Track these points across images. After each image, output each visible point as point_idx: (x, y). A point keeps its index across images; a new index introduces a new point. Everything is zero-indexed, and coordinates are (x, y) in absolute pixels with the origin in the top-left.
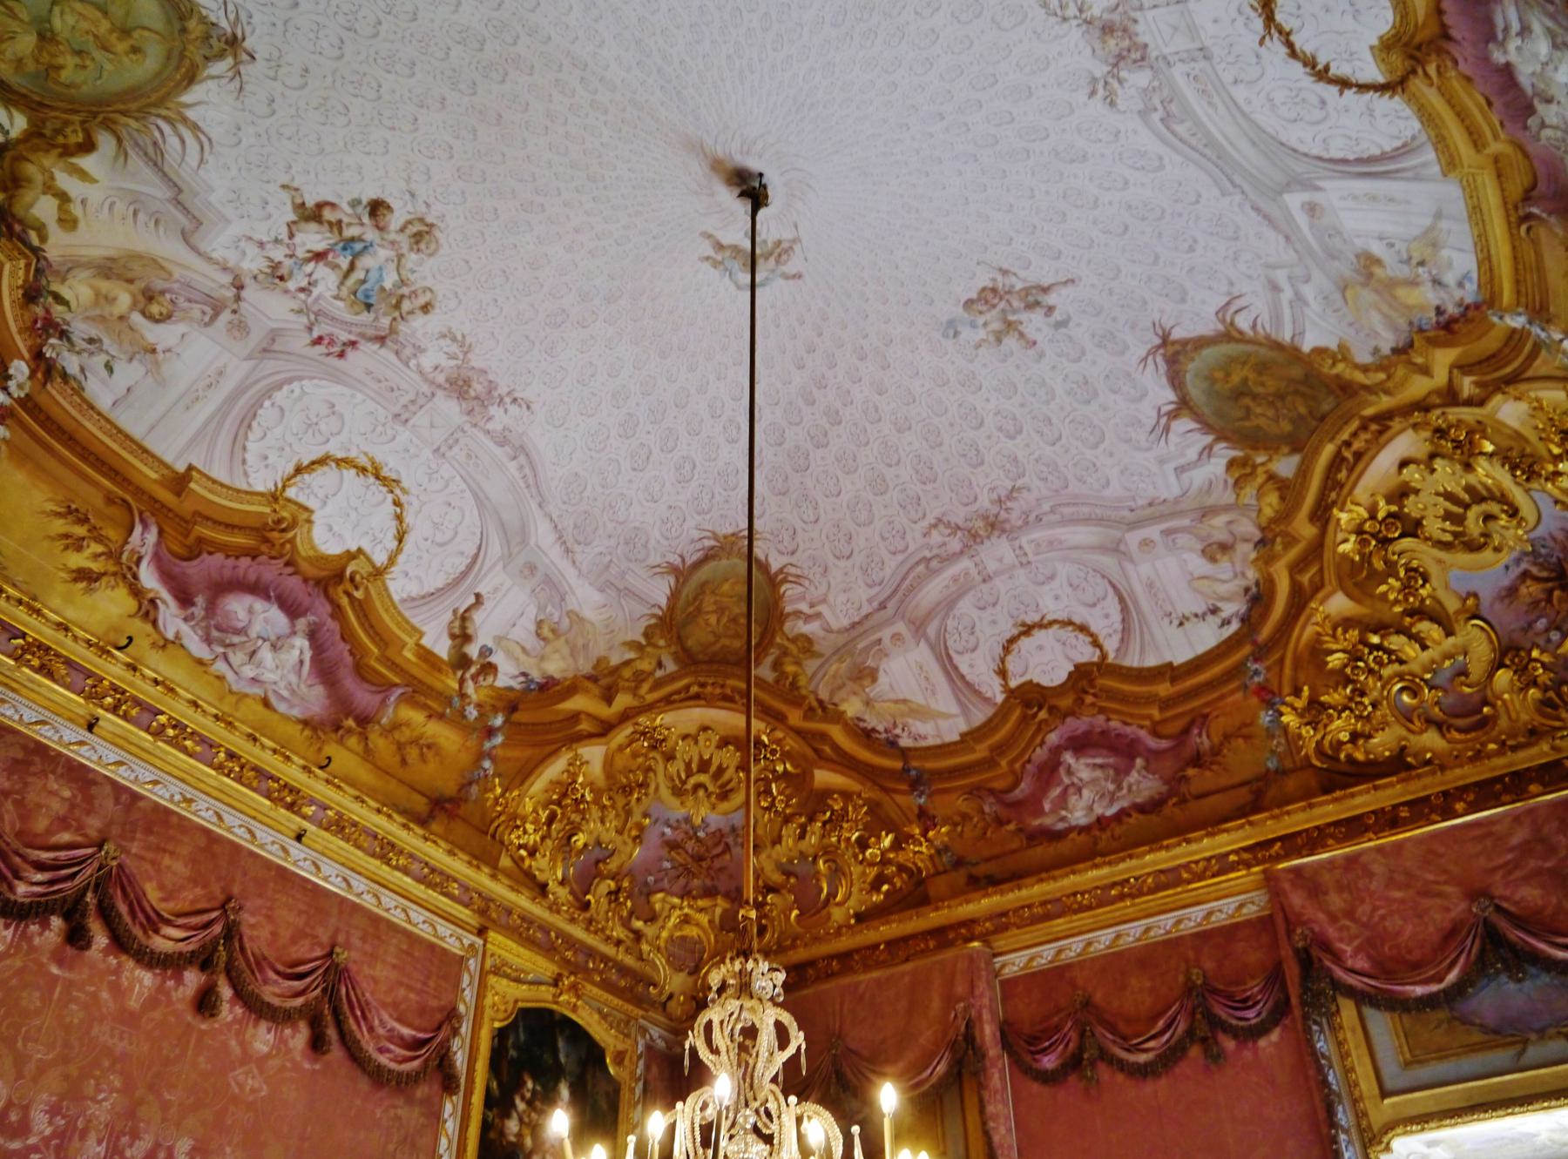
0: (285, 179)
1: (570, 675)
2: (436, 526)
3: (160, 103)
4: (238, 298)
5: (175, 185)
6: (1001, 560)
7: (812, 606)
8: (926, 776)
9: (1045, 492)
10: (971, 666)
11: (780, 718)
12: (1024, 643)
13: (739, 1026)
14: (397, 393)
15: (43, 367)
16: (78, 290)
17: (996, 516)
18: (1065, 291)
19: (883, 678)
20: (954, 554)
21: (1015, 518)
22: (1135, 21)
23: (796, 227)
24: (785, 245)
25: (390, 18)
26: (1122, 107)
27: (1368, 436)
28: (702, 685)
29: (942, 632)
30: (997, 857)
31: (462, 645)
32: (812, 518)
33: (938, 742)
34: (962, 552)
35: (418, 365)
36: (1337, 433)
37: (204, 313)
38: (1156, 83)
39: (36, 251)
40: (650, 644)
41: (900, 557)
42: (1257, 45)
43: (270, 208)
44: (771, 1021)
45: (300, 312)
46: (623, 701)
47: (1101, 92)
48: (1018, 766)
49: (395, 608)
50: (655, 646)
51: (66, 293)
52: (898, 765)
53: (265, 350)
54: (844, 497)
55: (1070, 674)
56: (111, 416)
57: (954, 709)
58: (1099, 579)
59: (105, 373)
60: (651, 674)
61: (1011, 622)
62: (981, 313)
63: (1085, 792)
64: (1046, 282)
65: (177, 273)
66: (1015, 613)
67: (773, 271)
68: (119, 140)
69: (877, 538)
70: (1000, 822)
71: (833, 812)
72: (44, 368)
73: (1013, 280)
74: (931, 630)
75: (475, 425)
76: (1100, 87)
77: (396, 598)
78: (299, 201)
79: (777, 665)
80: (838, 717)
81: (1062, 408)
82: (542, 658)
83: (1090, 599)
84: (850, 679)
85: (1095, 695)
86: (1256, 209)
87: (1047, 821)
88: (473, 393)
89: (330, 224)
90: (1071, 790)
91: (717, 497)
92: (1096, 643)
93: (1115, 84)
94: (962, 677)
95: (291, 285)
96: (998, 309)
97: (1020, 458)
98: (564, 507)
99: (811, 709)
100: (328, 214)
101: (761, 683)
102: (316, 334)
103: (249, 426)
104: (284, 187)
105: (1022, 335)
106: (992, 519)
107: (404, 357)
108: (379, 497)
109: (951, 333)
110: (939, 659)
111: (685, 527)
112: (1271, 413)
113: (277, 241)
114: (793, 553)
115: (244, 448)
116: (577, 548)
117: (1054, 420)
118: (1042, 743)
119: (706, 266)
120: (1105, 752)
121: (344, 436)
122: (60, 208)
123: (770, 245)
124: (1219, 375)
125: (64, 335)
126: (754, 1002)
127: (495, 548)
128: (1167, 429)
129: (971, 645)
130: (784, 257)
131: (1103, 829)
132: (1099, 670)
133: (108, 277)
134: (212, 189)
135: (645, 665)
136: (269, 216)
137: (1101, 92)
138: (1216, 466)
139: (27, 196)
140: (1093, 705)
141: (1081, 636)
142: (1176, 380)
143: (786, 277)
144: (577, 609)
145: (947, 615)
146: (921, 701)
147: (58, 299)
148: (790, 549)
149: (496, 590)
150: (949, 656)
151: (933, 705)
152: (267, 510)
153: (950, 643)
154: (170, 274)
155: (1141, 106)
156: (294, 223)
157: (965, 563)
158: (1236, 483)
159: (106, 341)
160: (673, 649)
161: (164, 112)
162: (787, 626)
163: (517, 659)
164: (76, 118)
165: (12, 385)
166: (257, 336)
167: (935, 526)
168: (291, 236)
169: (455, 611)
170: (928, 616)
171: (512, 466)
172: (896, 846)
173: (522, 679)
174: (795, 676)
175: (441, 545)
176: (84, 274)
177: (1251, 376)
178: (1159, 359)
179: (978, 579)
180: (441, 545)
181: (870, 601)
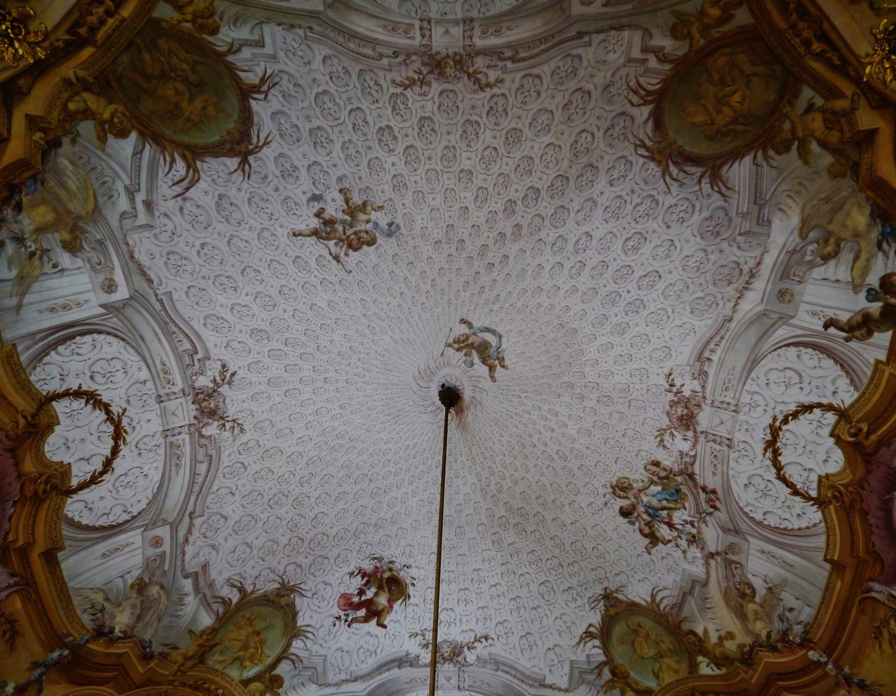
0: (646, 555)
1: (862, 196)
2: (788, 386)
3: (653, 611)
4: (718, 554)
5: (684, 596)
6: (447, 32)
7: (644, 61)
9: (381, 74)
14: (716, 453)
15: (806, 643)
16: (760, 628)
17: (431, 72)
18: (302, 227)
20: (485, 55)
21: (416, 63)
22: (195, 417)
23: (442, 354)
24: (456, 346)
25: (542, 557)
26: (219, 363)
27: (91, 19)
28: (807, 43)
31: (874, 321)
32: (584, 135)
34: (478, 53)
35: (691, 450)
36: (118, 27)
37: (736, 568)
38: (194, 378)
39: (752, 648)
40: (794, 136)
41: (535, 71)
42: (128, 408)
43: (664, 555)
45: (705, 522)
47: (228, 375)
50: (793, 129)
51: (764, 633)
53: (737, 532)
54: (547, 140)
56: (817, 607)
59: (795, 612)
60: (823, 110)
62: (367, 232)
64: (312, 240)
65: (724, 585)
67: (474, 334)
68: (681, 622)
69: (543, 95)
72: (806, 643)
73: (334, 250)
75: (704, 397)
76: (228, 378)
77: (856, 395)
78: (651, 545)
79: (726, 18)
81: (340, 132)
82: (856, 235)
86: (150, 281)
88: (686, 411)
89: (650, 528)
91: (637, 200)
93: (218, 378)
95: (694, 531)
96: (354, 229)
97: (390, 109)
98: (721, 303)
100: (647, 530)
102: (712, 510)
103: (785, 529)
104: (649, 554)
105: (347, 201)
106: (437, 71)
107: (692, 460)
108: (788, 435)
109: (393, 228)
111: (674, 201)
112: (175, 60)
113: (677, 546)
115: (800, 529)
116: (746, 269)
117: (350, 126)
119: (507, 363)
121: (759, 472)
122: (727, 640)
123: (464, 351)
124: (211, 110)
125: (785, 633)
127: (782, 333)
128: (263, 80)
130: (462, 338)
133: (746, 616)
134: (675, 581)
135: (817, 124)
136: (668, 554)
137: (228, 375)
138: (227, 35)
139: (729, 653)
142: (247, 117)
143: (470, 325)
144: (796, 232)
147: (769, 636)
148: (622, 118)
149: (814, 314)
152: (832, 507)
154: (726, 588)
155: (207, 363)
156: (662, 543)
157: (480, 42)
158: (212, 15)
159: (778, 613)
160: (787, 109)
161: (656, 609)
163: (868, 260)
164: (684, 640)
165: (823, 659)
166: (732, 539)
167: (489, 85)
168: (670, 541)
169: (848, 340)
171: (715, 358)
173: (885, 246)
175: (800, 376)
176: (751, 627)
177: (184, 104)
178: (255, 140)
179: (476, 25)
180: (800, 376)
181: (589, 44)
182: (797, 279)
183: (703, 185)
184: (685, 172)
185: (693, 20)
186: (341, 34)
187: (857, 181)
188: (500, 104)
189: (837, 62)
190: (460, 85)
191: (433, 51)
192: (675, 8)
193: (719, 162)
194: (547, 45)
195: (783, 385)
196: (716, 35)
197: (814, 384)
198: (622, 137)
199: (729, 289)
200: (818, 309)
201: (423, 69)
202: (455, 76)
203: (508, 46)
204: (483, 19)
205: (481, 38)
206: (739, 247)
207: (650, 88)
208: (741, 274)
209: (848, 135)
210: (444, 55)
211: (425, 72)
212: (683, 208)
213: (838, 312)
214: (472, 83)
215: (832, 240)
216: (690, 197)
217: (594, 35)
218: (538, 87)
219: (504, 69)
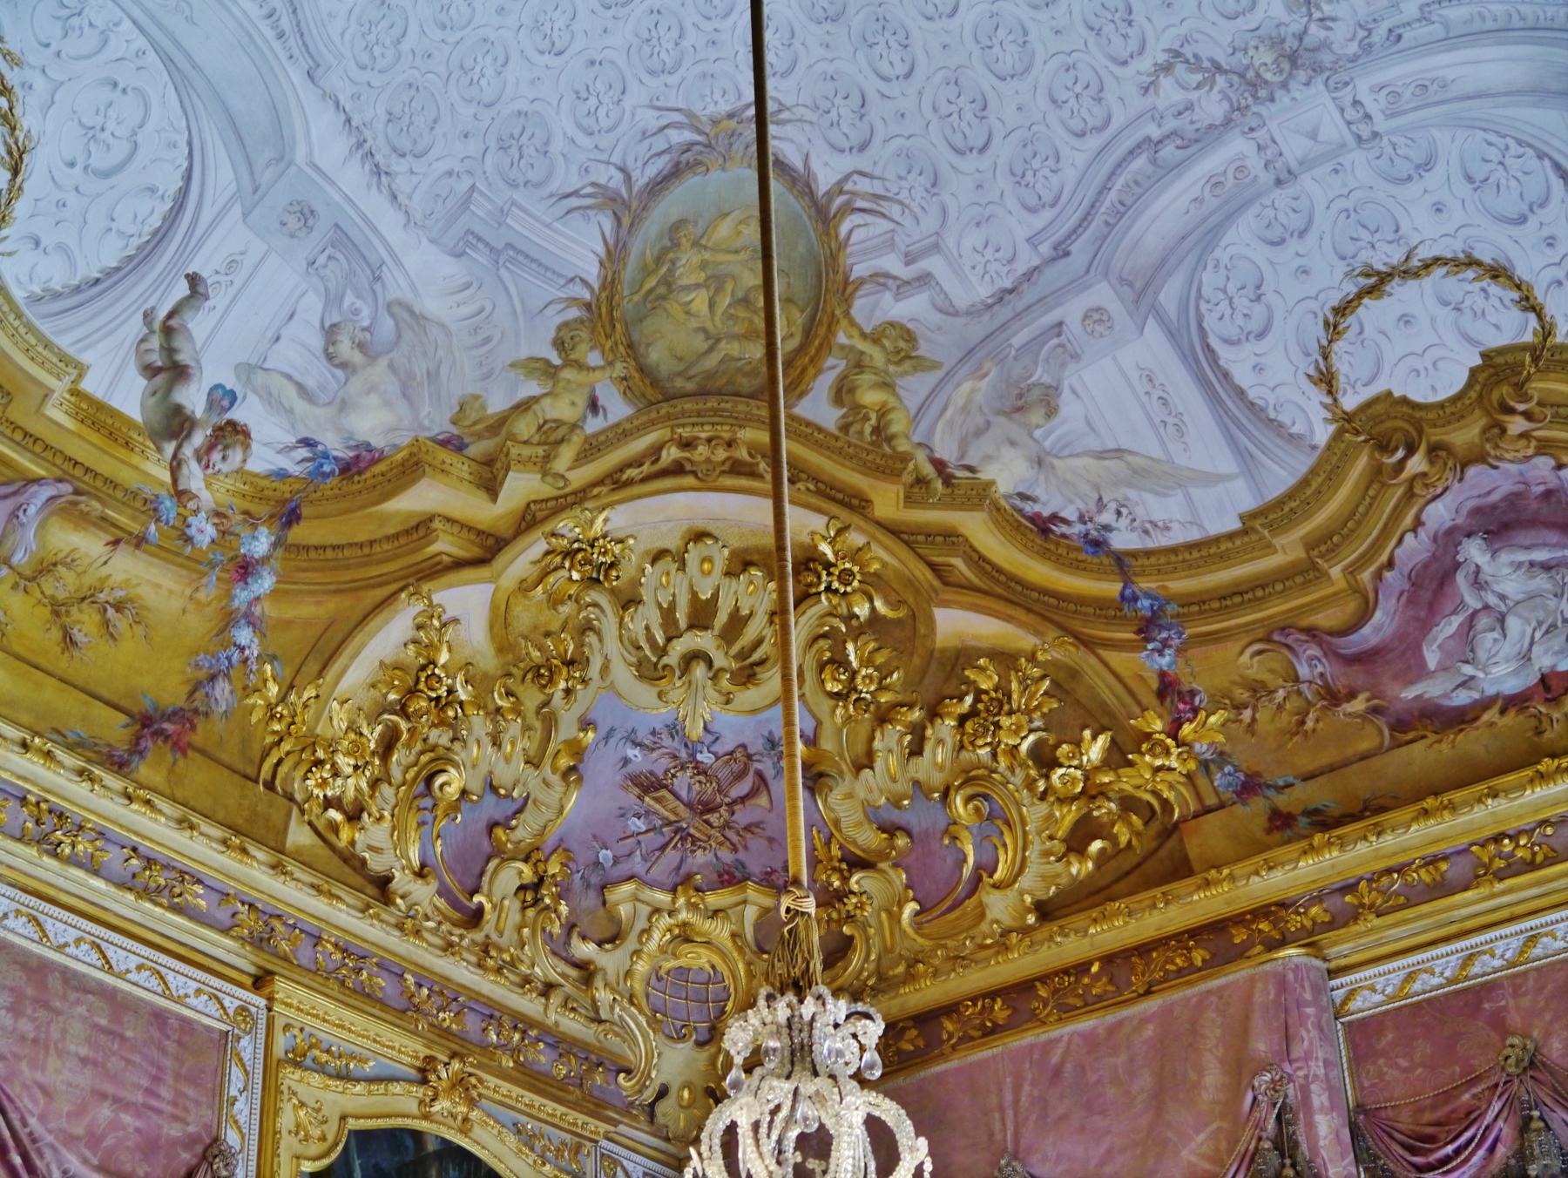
1: (404, 439)
2: (91, 133)
6: (1313, 135)
7: (909, 259)
8: (1171, 609)
10: (1258, 368)
11: (856, 503)
12: (1370, 311)
13: (793, 1134)
17: (1300, 37)
19: (1070, 408)
21: (1342, 38)
28: (687, 444)
29: (1192, 297)
30: (1332, 769)
31: (169, 389)
32: (901, 69)
33: (1195, 535)
34: (1228, 122)
40: (569, 363)
41: (1094, 142)
44: (858, 1118)
46: (521, 487)
48: (1366, 576)
49: (19, 316)
50: (580, 366)
52: (1112, 588)
55: (1474, 372)
57: (1226, 463)
58: (1533, 163)
61: (1341, 268)
63: (1513, 623)
66: (1350, 249)
69: (1043, 102)
70: (1333, 697)
71: (979, 693)
74: (1169, 296)
77: (18, 294)
79: (842, 393)
80: (979, 495)
82: (343, 406)
83: (1510, 204)
84: (1000, 412)
85: (1528, 415)
87: (1432, 689)
90: (1483, 621)
91: (692, 37)
92: (1529, 304)
94: (1241, 393)
98: (363, 76)
99: (921, 481)
101: (806, 431)
106: (1291, 43)
110: (1189, 358)
111: (628, 103)
114: (863, 147)
116: (399, 166)
118: (1418, 523)
120: (1553, 537)
126: (822, 1083)
127: (221, 176)
129: (1255, 325)
131: (1554, 701)
132: (1536, 360)
135: (562, 408)
140: (1524, 435)
141: (1494, 289)
144: (408, 296)
145: (1200, 263)
146: (1157, 453)
148: (856, 139)
149: (232, 265)
150: (1208, 349)
151: (1181, 460)
153: (1210, 322)
157: (1237, 145)
160: (619, 369)
162: (859, 308)
167: (1166, 68)
169: (148, 316)
170: (1161, 267)
172: (1117, 757)
173: (304, 452)
174: (883, 412)
175: (106, 174)
179: (1266, 178)
180: (106, 174)
181: (1033, 241)
182: (322, 259)
183: (613, 171)
184: (659, 154)
185: (892, 368)
186: (1530, 22)
187: (433, 440)
188: (1117, 41)
189: (632, 473)
190: (1226, 39)
191: (1319, 81)
192: (939, 374)
193: (626, 221)
194: (1107, 204)
195: (98, 121)
196: (830, 361)
197: (71, 198)
198: (824, 105)
199: (381, 110)
200: (239, 279)
201: (1322, 34)
202: (1245, 50)
203: (1178, 167)
204: (1258, 196)
205: (1242, 157)
206: (450, 173)
207: (856, 219)
208: (394, 150)
209: (514, 452)
210: (1293, 85)
211: (1314, 29)
212: (601, 113)
213: (216, 315)
214: (1203, 56)
215: (357, 357)
216: (612, 136)
217: (1036, 262)
218: (1065, 113)
219: (1157, 116)
